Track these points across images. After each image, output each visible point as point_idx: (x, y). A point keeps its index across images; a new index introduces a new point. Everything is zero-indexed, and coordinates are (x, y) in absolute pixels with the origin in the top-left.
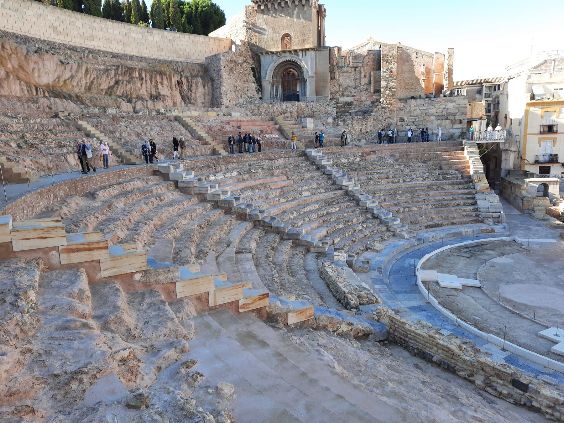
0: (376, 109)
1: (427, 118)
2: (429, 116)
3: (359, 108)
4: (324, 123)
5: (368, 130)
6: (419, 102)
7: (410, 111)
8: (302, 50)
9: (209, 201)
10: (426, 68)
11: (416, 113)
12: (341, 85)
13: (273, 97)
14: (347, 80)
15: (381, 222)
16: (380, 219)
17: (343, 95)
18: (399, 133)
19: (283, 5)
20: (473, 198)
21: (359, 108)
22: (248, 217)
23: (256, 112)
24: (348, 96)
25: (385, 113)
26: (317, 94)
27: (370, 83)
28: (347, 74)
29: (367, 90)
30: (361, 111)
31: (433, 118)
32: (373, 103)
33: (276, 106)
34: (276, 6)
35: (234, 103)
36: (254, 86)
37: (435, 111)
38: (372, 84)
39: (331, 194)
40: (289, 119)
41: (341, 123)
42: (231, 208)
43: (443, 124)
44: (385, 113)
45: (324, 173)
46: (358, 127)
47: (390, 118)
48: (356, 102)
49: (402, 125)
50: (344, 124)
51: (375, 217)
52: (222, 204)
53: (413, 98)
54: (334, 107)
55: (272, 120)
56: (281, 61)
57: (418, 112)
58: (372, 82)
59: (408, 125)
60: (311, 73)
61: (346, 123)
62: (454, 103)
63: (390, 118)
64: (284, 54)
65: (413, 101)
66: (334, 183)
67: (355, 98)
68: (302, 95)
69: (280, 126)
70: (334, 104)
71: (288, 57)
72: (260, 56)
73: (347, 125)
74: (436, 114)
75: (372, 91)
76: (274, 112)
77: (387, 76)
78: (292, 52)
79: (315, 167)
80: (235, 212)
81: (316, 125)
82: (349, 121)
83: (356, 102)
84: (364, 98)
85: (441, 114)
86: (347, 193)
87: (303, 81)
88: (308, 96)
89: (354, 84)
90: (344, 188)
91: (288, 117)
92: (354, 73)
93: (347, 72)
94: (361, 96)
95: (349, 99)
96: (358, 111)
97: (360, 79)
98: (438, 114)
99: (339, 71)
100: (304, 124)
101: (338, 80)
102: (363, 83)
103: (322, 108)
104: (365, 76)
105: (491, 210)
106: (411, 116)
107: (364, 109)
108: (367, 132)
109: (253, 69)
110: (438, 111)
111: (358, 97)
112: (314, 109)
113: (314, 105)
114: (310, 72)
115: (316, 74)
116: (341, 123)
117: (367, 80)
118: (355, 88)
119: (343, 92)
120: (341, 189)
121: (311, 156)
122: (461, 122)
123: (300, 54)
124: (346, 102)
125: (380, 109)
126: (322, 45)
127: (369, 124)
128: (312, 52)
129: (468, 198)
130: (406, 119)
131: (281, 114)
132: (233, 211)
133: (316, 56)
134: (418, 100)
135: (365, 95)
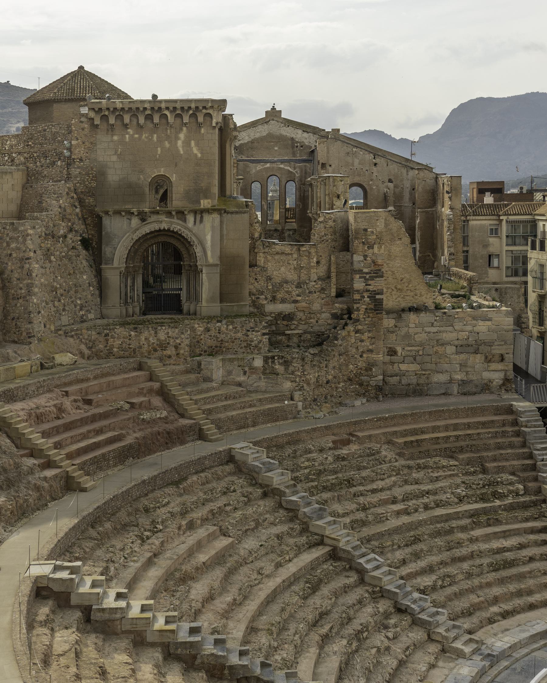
0: (344, 333)
1: (440, 349)
2: (442, 345)
3: (306, 327)
4: (247, 369)
5: (330, 377)
6: (424, 317)
7: (407, 336)
9: (153, 645)
10: (395, 187)
11: (418, 338)
12: (269, 279)
13: (126, 303)
14: (283, 269)
15: (416, 622)
16: (412, 615)
17: (274, 299)
18: (387, 379)
21: (306, 327)
22: (226, 672)
23: (101, 346)
24: (283, 301)
25: (362, 341)
26: (223, 297)
27: (329, 277)
28: (283, 257)
29: (323, 290)
30: (310, 333)
31: (450, 349)
32: (335, 316)
33: (146, 334)
35: (53, 328)
36: (86, 278)
37: (454, 335)
38: (334, 280)
39: (307, 557)
40: (172, 361)
41: (279, 368)
42: (195, 657)
43: (470, 363)
44: (362, 341)
45: (280, 506)
46: (312, 377)
47: (371, 351)
48: (300, 315)
49: (392, 363)
50: (286, 369)
51: (400, 610)
52: (177, 649)
53: (411, 309)
54: (264, 334)
55: (140, 367)
56: (147, 229)
57: (421, 337)
58: (333, 275)
59: (403, 362)
60: (212, 256)
61: (291, 368)
62: (489, 323)
63: (371, 351)
64: (154, 218)
65: (412, 317)
66: (305, 529)
67: (297, 305)
68: (188, 299)
69: (163, 386)
70: (265, 327)
71: (164, 223)
72: (100, 218)
73: (293, 373)
74: (456, 343)
75: (333, 294)
76: (140, 347)
77: (366, 270)
78: (174, 213)
79: (260, 491)
80: (203, 663)
81: (230, 373)
82: (296, 364)
83: (300, 315)
84: (316, 306)
85: (465, 342)
86: (335, 555)
87: (196, 271)
88: (204, 304)
89: (295, 277)
90: (326, 540)
91: (170, 357)
92: (295, 256)
93: (283, 253)
94: (311, 303)
95: (286, 308)
96: (305, 332)
97: (309, 268)
98: (460, 343)
99: (266, 250)
100: (205, 373)
101: (264, 269)
102: (314, 277)
103: (239, 335)
104: (318, 263)
106: (409, 345)
107: (316, 328)
108: (328, 382)
109: (85, 243)
110: (460, 337)
111: (304, 304)
112: (222, 336)
113: (223, 328)
114: (209, 254)
115: (221, 258)
116: (279, 368)
117: (322, 271)
118: (299, 286)
119: (275, 292)
120: (321, 543)
121: (245, 463)
122: (502, 359)
124: (280, 314)
125: (352, 334)
126: (228, 193)
127: (331, 365)
128: (216, 216)
130: (399, 349)
131: (155, 350)
132: (198, 661)
133: (221, 222)
134: (422, 314)
135: (319, 300)
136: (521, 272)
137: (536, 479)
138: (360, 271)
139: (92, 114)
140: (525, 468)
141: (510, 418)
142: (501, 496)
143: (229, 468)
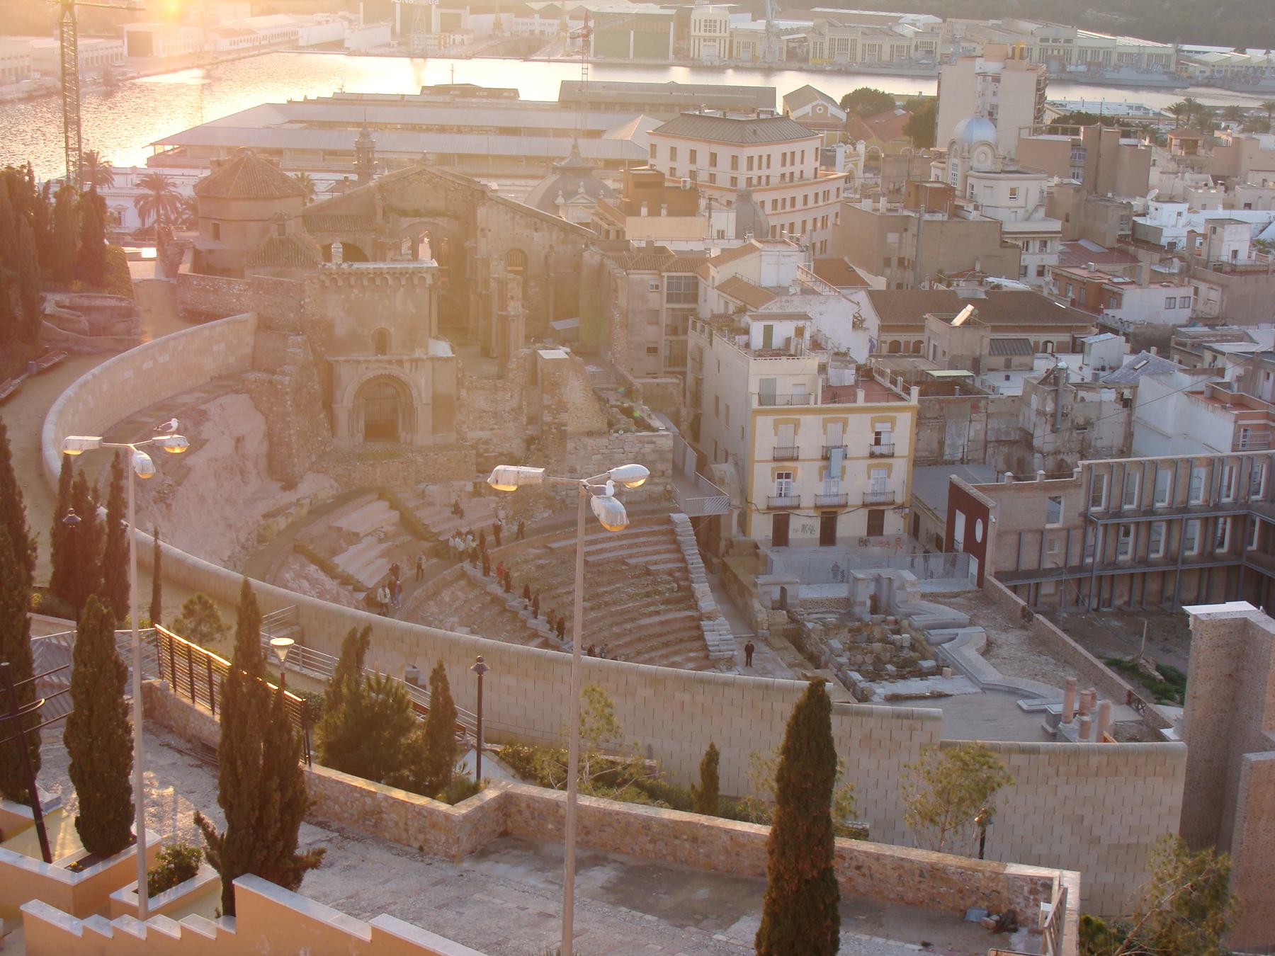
8: (412, 361)
19: (378, 282)
20: (699, 628)
24: (482, 429)
34: (366, 283)
45: (505, 610)
83: (495, 440)
105: (722, 648)
114: (423, 394)
123: (407, 366)
129: (691, 628)
130: (578, 468)
136: (680, 330)
137: (687, 579)
138: (548, 407)
139: (323, 277)
140: (680, 569)
141: (668, 527)
142: (660, 593)
143: (463, 583)
